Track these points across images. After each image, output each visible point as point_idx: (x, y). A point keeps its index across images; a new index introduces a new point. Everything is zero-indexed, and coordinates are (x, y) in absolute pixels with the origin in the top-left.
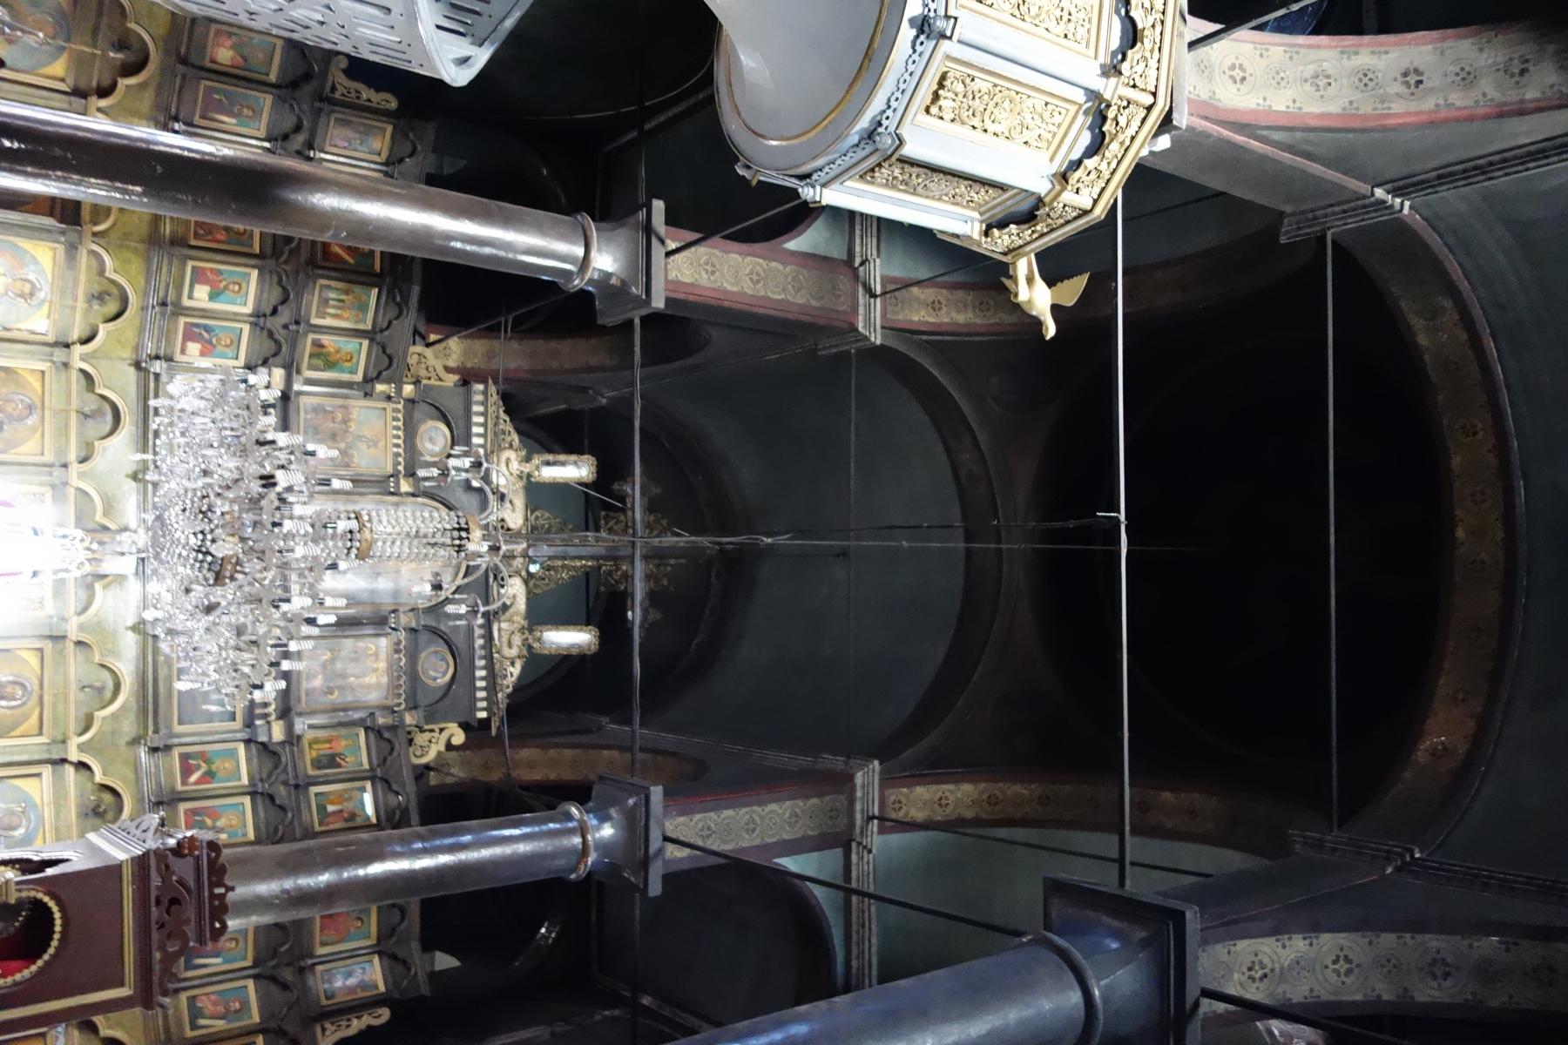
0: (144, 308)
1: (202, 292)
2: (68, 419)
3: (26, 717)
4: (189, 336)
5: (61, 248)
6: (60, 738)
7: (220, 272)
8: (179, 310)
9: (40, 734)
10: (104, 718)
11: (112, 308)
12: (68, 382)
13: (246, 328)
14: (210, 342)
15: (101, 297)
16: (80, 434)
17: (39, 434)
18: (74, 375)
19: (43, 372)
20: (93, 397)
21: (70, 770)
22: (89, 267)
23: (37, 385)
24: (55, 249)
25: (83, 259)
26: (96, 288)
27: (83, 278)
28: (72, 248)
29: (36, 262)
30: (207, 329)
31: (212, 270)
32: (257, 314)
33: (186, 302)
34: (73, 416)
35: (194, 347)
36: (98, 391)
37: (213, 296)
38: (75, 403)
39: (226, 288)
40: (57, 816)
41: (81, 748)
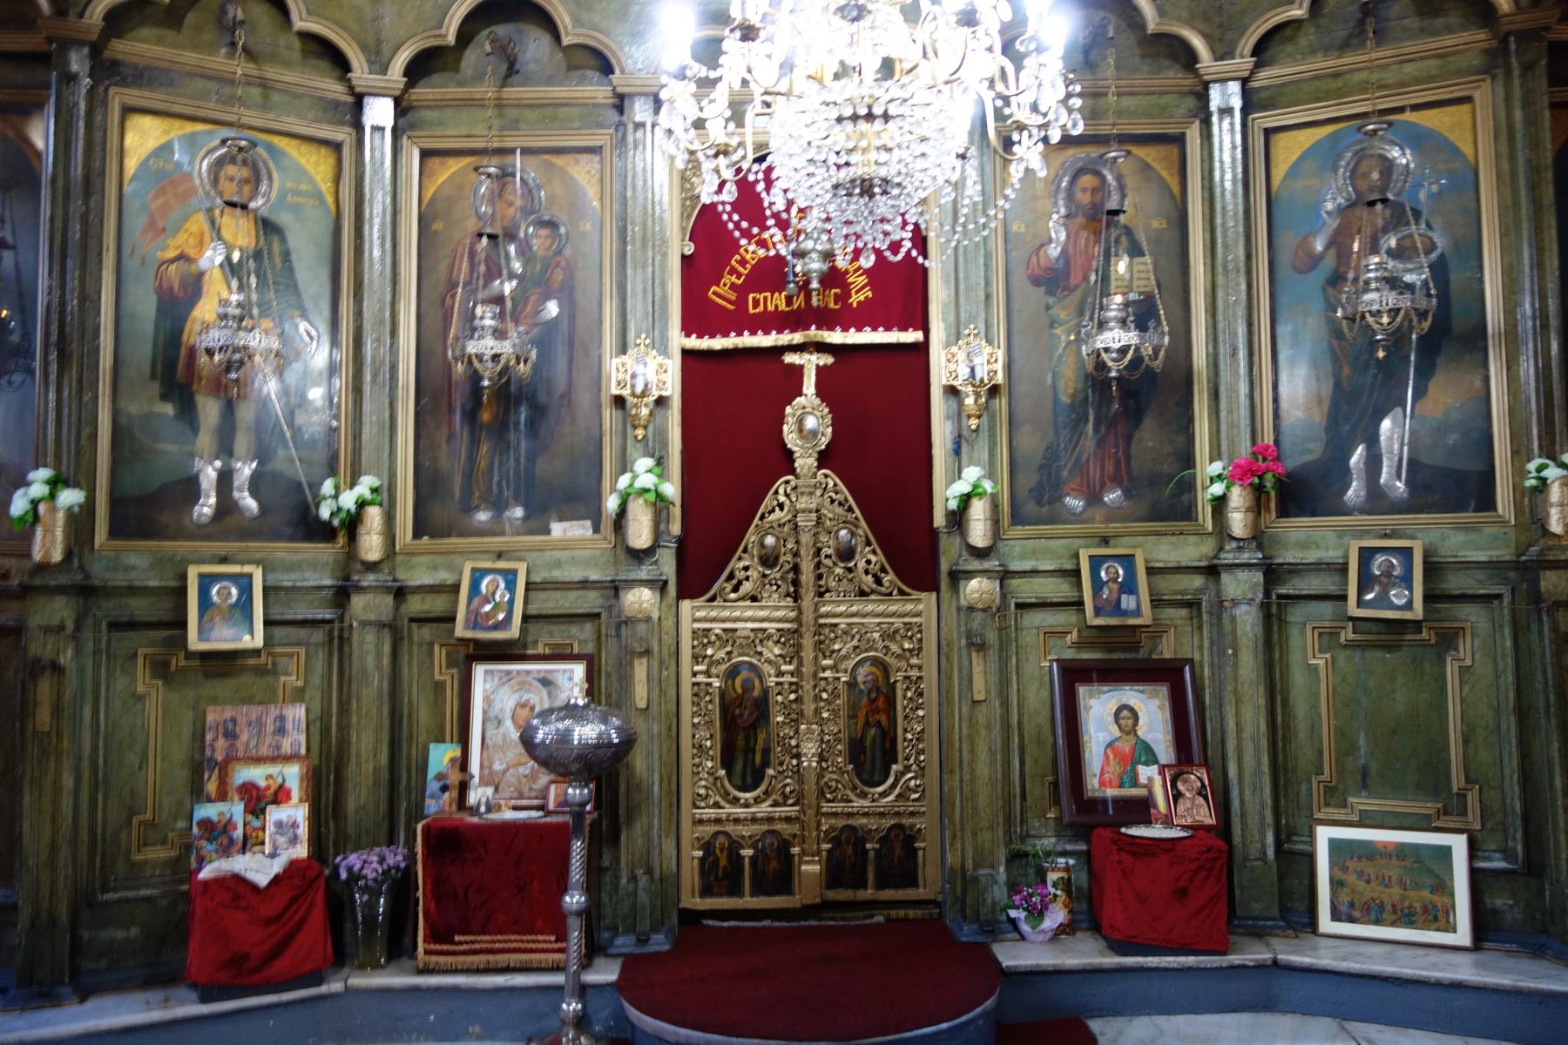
2: (519, 105)
3: (1146, 167)
5: (118, 97)
6: (1190, 102)
9: (1179, 140)
10: (1162, 12)
12: (441, 104)
16: (550, 81)
17: (559, 161)
18: (421, 92)
19: (426, 154)
20: (471, 57)
21: (1266, 77)
22: (160, 41)
23: (455, 165)
24: (128, 110)
27: (190, 57)
28: (106, 70)
29: (164, 150)
34: (511, 92)
36: (451, 39)
38: (487, 90)
40: (1364, 87)
41: (1223, 52)
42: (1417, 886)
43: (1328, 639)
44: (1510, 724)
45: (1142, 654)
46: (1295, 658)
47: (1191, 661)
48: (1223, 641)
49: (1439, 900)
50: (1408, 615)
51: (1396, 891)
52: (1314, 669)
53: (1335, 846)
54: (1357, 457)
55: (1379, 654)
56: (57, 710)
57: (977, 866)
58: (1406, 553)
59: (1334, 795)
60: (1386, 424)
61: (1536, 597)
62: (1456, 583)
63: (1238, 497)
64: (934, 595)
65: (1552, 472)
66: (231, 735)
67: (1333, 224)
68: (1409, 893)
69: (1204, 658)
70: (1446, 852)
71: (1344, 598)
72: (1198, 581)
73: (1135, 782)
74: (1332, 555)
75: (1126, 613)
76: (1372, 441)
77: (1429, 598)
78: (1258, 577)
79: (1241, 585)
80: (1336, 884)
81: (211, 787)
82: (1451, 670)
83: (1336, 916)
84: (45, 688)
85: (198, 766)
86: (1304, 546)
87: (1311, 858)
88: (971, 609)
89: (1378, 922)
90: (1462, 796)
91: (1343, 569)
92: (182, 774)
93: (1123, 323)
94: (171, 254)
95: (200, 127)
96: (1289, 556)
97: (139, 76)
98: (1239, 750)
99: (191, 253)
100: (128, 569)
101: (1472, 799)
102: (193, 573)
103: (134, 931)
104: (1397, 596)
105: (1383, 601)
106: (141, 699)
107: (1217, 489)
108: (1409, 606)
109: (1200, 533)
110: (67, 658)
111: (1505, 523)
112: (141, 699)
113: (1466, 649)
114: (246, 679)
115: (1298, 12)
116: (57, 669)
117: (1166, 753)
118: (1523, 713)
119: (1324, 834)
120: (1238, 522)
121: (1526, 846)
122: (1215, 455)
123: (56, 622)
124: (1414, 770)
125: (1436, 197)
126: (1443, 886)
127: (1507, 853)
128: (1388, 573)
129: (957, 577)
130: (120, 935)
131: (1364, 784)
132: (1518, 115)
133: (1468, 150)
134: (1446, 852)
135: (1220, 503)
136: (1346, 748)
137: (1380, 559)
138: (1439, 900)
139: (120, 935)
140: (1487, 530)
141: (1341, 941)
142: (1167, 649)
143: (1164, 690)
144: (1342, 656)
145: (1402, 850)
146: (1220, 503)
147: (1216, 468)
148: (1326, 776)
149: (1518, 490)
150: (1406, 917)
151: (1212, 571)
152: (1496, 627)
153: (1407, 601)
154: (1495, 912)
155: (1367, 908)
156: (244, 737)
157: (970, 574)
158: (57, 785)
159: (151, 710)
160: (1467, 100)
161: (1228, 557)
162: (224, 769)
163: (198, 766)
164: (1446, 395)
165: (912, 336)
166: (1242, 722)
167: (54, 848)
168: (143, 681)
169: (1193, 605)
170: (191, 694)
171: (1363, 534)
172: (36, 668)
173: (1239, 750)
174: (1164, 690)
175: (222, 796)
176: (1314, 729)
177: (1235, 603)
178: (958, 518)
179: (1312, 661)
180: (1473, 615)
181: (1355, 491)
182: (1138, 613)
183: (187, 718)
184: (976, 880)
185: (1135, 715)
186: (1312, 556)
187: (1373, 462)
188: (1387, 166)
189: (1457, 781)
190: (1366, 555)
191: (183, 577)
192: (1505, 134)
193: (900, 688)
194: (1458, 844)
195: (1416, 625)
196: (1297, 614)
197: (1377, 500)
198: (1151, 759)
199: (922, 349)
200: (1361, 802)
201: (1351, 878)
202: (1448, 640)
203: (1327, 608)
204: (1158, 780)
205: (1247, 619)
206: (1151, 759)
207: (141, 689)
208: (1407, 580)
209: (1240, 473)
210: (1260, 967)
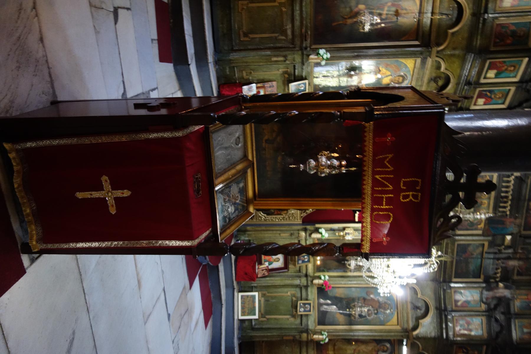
0: (458, 84)
1: (491, 74)
4: (480, 96)
5: (419, 60)
7: (505, 62)
8: (478, 84)
11: (440, 83)
13: (513, 89)
14: (491, 98)
15: (435, 80)
25: (430, 62)
26: (434, 75)
29: (406, 66)
30: (490, 91)
31: (500, 62)
32: (521, 81)
33: (482, 81)
35: (481, 101)
37: (497, 76)
39: (506, 70)
42: (248, 310)
43: (294, 295)
44: (279, 326)
45: (290, 262)
46: (289, 289)
47: (288, 270)
48: (293, 277)
49: (246, 314)
50: (298, 311)
51: (247, 306)
52: (287, 293)
53: (254, 297)
54: (329, 302)
55: (290, 304)
56: (276, 61)
57: (248, 234)
58: (310, 311)
59: (264, 295)
60: (335, 307)
61: (302, 332)
62: (304, 319)
63: (321, 282)
64: (301, 223)
65: (324, 337)
66: (270, 87)
67: (376, 299)
68: (248, 309)
69: (289, 274)
70: (255, 314)
71: (301, 300)
72: (304, 272)
73: (265, 262)
74: (310, 297)
75: (298, 261)
76: (332, 304)
77: (301, 315)
78: (305, 284)
79: (304, 281)
80: (248, 296)
81: (259, 85)
82: (288, 317)
83: (242, 296)
84: (281, 59)
85: (263, 81)
86: (311, 292)
87: (252, 291)
88: (299, 234)
89: (242, 303)
90: (265, 317)
91: (307, 300)
92: (261, 77)
93: (357, 265)
94: (381, 69)
95: (412, 73)
96: (309, 289)
97: (423, 62)
98: (272, 280)
99: (381, 72)
100: (307, 68)
101: (265, 319)
102: (307, 81)
103: (228, 73)
104: (302, 310)
105: (301, 307)
106: (278, 70)
107: (323, 278)
108: (300, 312)
109: (314, 273)
110: (287, 62)
111: (315, 327)
112: (278, 70)
113: (292, 319)
114: (282, 87)
115: (419, 296)
116: (285, 61)
117: (271, 267)
118: (281, 329)
119: (256, 294)
120: (316, 281)
121: (257, 328)
122: (329, 277)
123: (296, 60)
124: (269, 309)
125: (379, 318)
126: (249, 314)
127: (255, 325)
128: (306, 308)
129: (305, 230)
130: (227, 71)
131: (267, 301)
132: (393, 334)
133: (389, 323)
134: (255, 314)
135: (320, 278)
136: (273, 298)
137: (309, 307)
138: (246, 314)
139: (227, 71)
140: (314, 324)
141: (239, 296)
142: (291, 266)
143: (283, 266)
144: (290, 298)
145: (254, 307)
146: (320, 278)
147: (327, 278)
148: (267, 294)
149: (322, 330)
150: (243, 308)
151: (306, 276)
152: (296, 325)
153: (301, 311)
154: (245, 322)
155: (244, 301)
156: (270, 89)
157: (306, 233)
158: (261, 62)
159: (276, 71)
160: (398, 325)
161: (309, 279)
162: (263, 87)
163: (263, 81)
164: (341, 319)
165: (357, 219)
166: (277, 281)
167: (247, 62)
168: (281, 71)
169: (300, 271)
170: (279, 78)
171: (314, 303)
172: (285, 56)
173: (272, 280)
174: (283, 266)
175: (257, 88)
176: (276, 292)
177: (300, 280)
178: (317, 231)
179: (289, 293)
180: (298, 321)
181: (322, 301)
182: (298, 263)
183: (274, 78)
184: (245, 234)
185: (278, 261)
186: (309, 293)
187: (328, 304)
188: (385, 309)
189: (268, 317)
190: (310, 304)
191: (306, 79)
192: (390, 331)
193: (282, 216)
194: (256, 317)
195: (297, 311)
196: (298, 290)
197: (320, 305)
198: (269, 264)
199: (354, 222)
200: (263, 300)
201: (249, 298)
202: (294, 316)
203: (299, 295)
204: (265, 266)
205: (297, 282)
206: (269, 264)
207: (280, 70)
208: (305, 311)
209: (325, 283)
210: (233, 286)
